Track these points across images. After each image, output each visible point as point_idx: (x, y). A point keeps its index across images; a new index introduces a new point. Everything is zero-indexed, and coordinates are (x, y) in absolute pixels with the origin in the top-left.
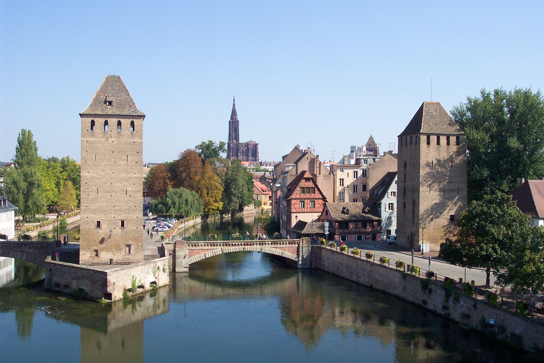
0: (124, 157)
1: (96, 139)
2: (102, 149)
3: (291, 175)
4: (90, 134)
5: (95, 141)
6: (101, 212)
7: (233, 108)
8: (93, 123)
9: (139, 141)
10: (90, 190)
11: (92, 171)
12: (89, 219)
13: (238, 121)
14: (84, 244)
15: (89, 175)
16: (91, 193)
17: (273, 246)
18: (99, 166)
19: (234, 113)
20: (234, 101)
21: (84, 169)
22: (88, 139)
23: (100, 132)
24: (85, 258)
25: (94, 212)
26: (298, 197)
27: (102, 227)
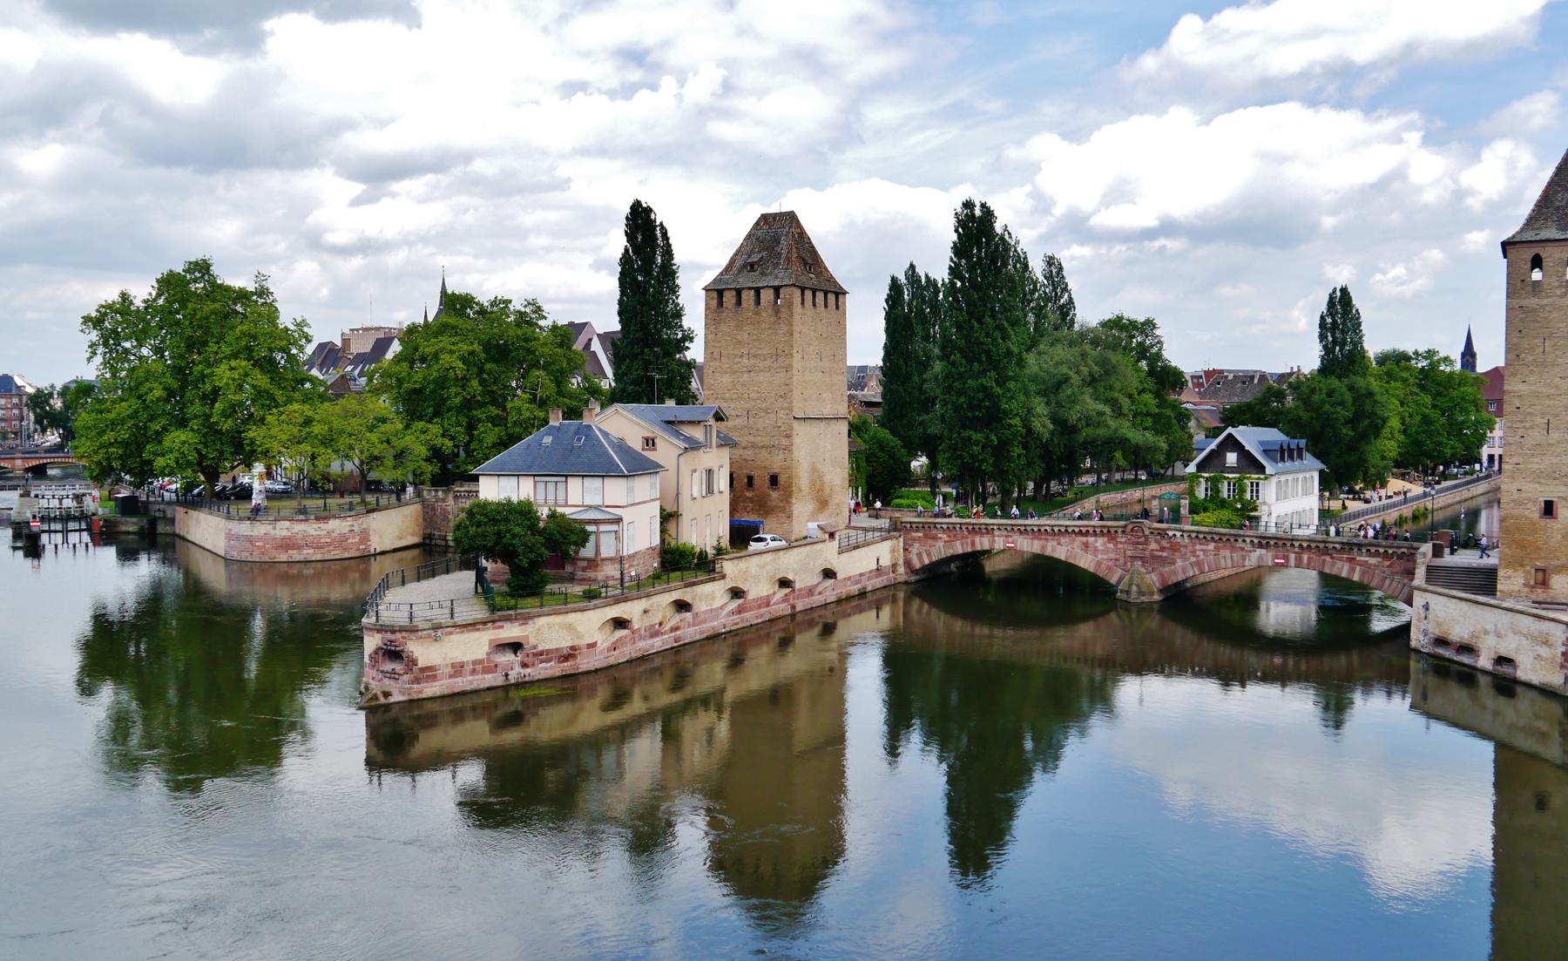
1: (1545, 301)
2: (1561, 325)
5: (1543, 307)
6: (1555, 479)
10: (1527, 425)
11: (1533, 378)
12: (1524, 495)
14: (1509, 553)
15: (1524, 388)
16: (1530, 432)
18: (1553, 366)
21: (1514, 374)
22: (1525, 302)
23: (1556, 284)
24: (1511, 587)
25: (1538, 477)
27: (1560, 516)
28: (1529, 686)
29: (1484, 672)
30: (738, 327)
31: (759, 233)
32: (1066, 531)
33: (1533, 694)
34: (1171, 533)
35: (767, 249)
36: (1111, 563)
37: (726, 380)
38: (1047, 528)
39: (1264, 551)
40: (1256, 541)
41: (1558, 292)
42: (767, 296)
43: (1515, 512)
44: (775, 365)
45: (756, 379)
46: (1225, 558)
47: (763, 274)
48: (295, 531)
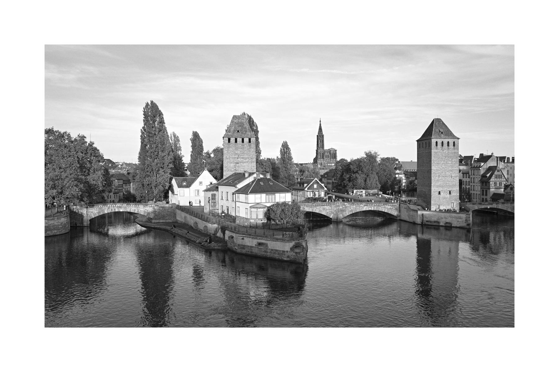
0: (450, 159)
1: (438, 151)
3: (483, 169)
4: (436, 148)
5: (438, 152)
7: (320, 127)
8: (437, 142)
9: (457, 151)
11: (436, 166)
12: (435, 190)
13: (323, 136)
17: (502, 205)
19: (320, 129)
20: (320, 122)
21: (433, 166)
25: (438, 186)
26: (494, 180)
28: (456, 227)
29: (442, 226)
30: (236, 149)
31: (235, 121)
32: (319, 205)
33: (458, 229)
34: (345, 204)
35: (240, 126)
36: (330, 212)
37: (232, 165)
38: (314, 205)
39: (366, 207)
40: (365, 204)
41: (440, 149)
42: (246, 140)
43: (434, 194)
44: (250, 161)
45: (243, 165)
46: (358, 209)
47: (242, 133)
48: (50, 223)
